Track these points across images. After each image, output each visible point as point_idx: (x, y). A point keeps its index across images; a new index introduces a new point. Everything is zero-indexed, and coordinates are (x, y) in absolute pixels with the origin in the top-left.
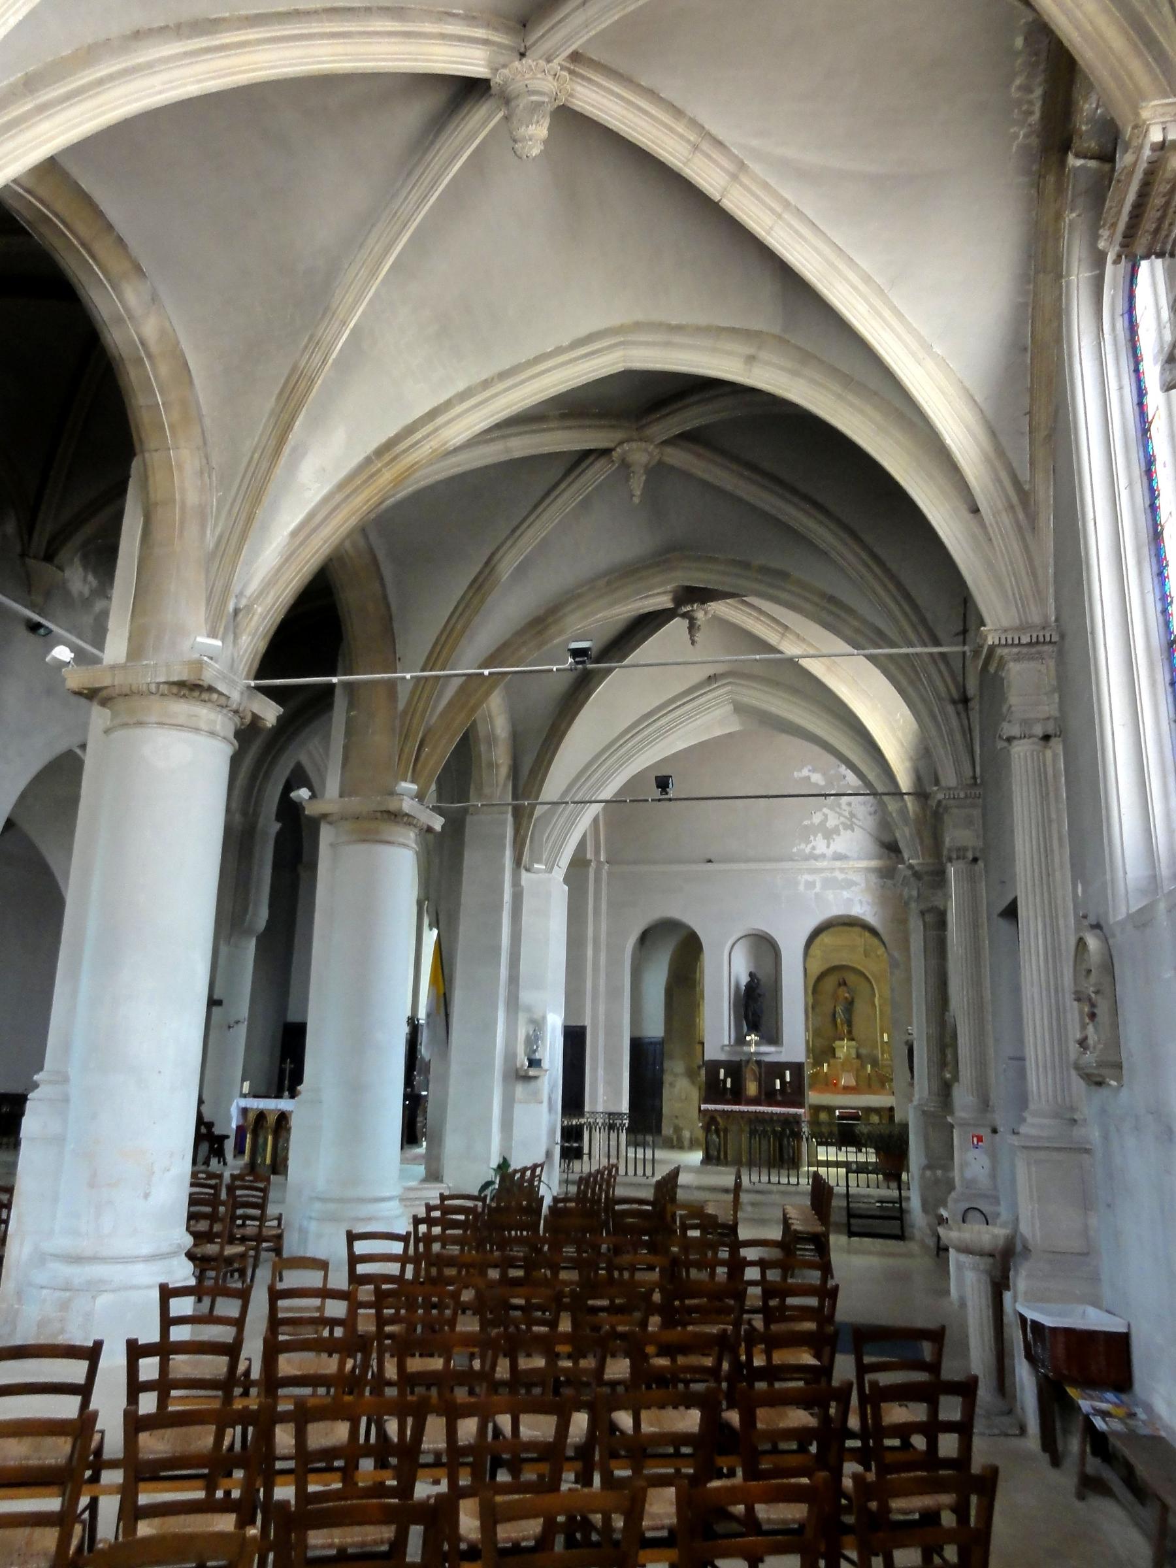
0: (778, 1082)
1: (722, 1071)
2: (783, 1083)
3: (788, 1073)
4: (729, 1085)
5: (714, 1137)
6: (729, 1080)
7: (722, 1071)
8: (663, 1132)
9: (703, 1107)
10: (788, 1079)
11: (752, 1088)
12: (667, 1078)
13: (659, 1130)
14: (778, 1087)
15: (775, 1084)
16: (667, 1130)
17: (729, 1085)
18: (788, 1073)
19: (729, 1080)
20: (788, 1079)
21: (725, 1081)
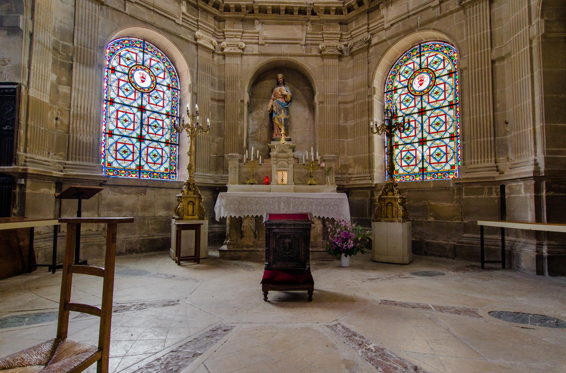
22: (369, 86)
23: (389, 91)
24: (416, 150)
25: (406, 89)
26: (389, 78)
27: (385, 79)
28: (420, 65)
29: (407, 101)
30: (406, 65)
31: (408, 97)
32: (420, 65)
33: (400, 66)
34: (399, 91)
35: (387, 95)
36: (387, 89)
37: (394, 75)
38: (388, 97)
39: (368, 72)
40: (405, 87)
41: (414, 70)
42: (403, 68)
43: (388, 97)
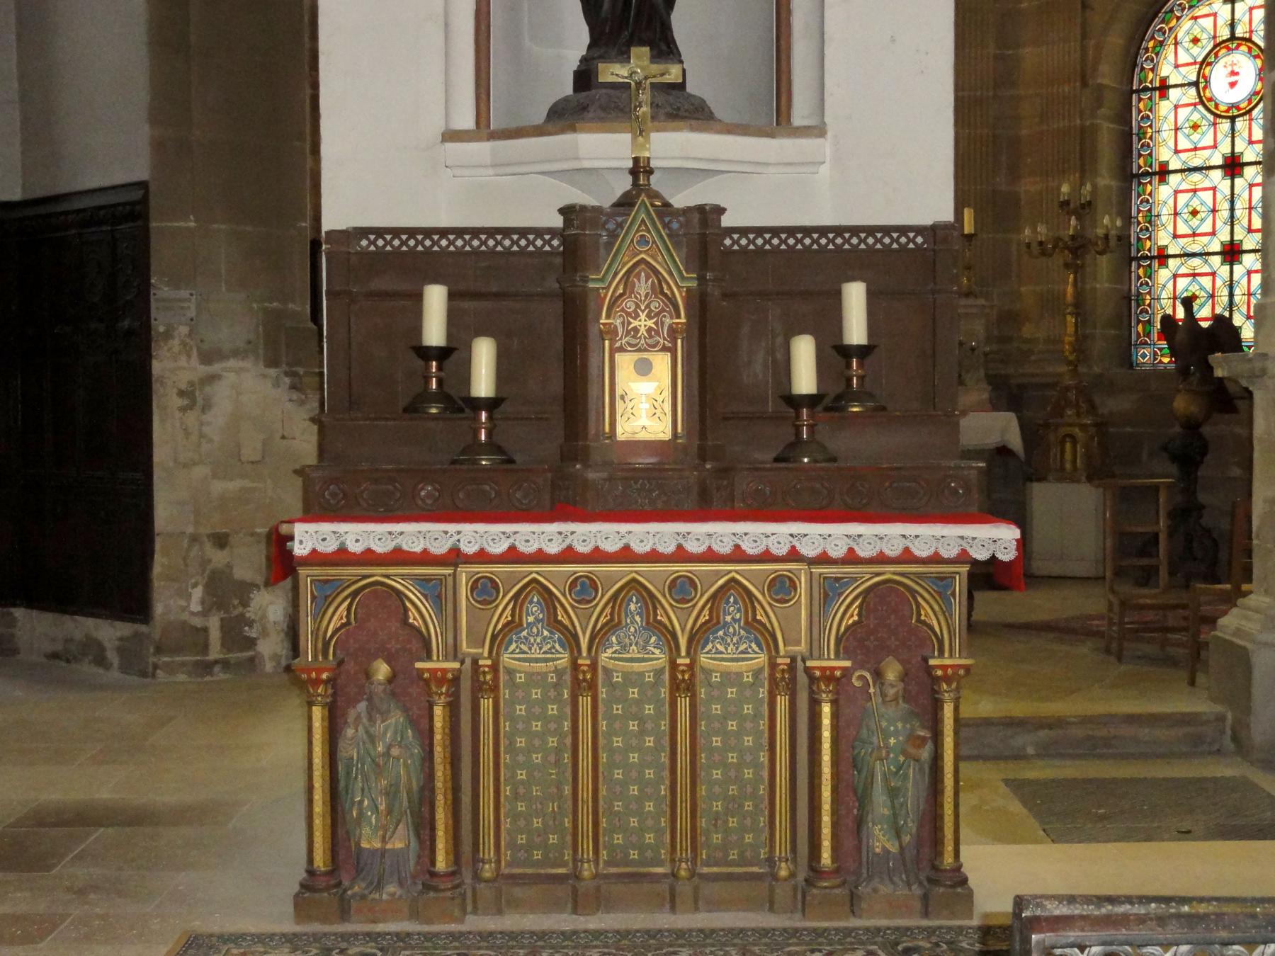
0: (804, 352)
1: (435, 298)
2: (835, 354)
3: (855, 296)
4: (483, 383)
5: (391, 727)
6: (484, 355)
7: (435, 298)
8: (159, 609)
9: (308, 538)
10: (856, 331)
11: (643, 401)
12: (171, 367)
13: (134, 604)
14: (805, 380)
15: (784, 368)
16: (177, 599)
17: (483, 383)
18: (855, 296)
19: (484, 355)
20: (856, 331)
21: (453, 355)
22: (1084, 84)
23: (1146, 89)
24: (1213, 274)
25: (1193, 91)
26: (1147, 50)
27: (1133, 50)
28: (1232, 26)
29: (1195, 127)
30: (1196, 18)
31: (1196, 117)
32: (1232, 26)
33: (1178, 18)
34: (1174, 94)
35: (1140, 100)
36: (1140, 82)
37: (1161, 43)
38: (1141, 105)
39: (1084, 36)
40: (1189, 84)
41: (1215, 37)
42: (1186, 24)
43: (1141, 105)
